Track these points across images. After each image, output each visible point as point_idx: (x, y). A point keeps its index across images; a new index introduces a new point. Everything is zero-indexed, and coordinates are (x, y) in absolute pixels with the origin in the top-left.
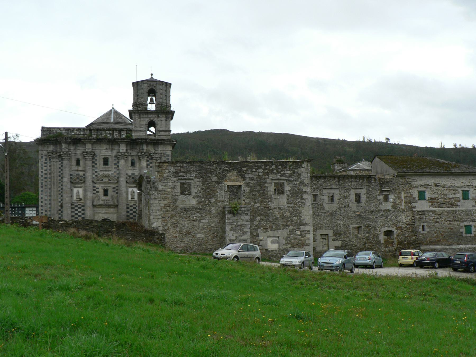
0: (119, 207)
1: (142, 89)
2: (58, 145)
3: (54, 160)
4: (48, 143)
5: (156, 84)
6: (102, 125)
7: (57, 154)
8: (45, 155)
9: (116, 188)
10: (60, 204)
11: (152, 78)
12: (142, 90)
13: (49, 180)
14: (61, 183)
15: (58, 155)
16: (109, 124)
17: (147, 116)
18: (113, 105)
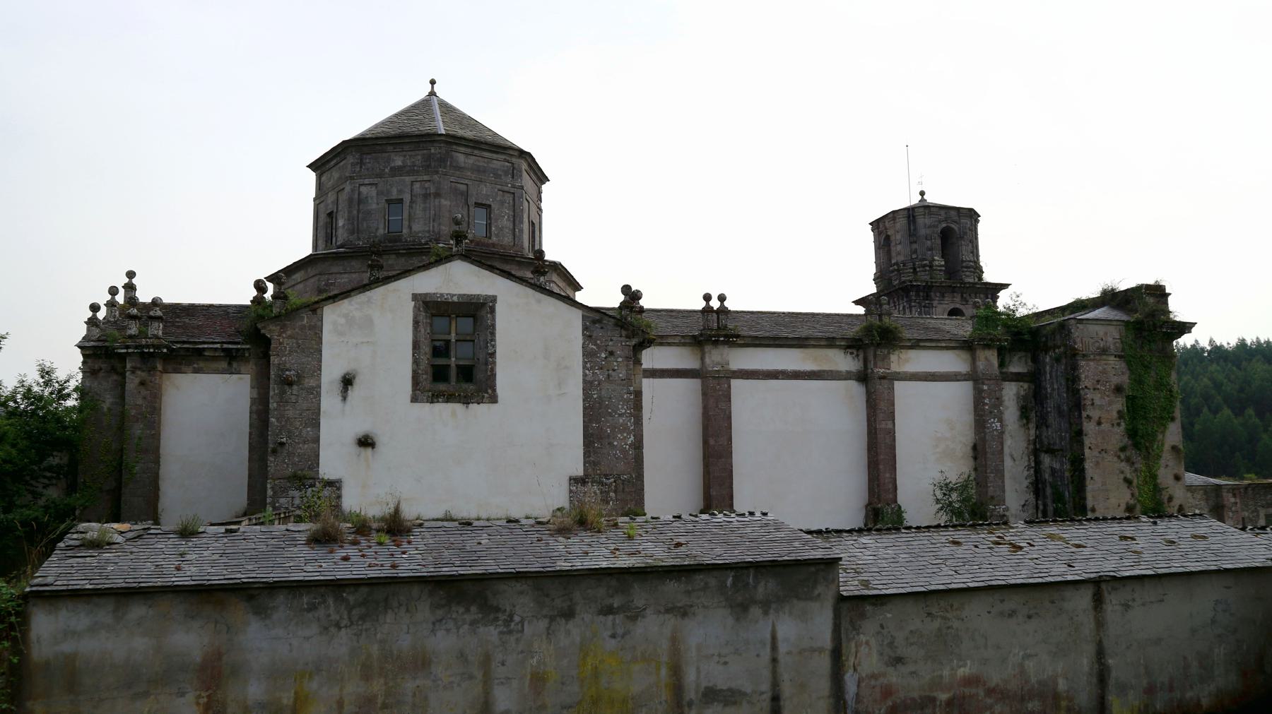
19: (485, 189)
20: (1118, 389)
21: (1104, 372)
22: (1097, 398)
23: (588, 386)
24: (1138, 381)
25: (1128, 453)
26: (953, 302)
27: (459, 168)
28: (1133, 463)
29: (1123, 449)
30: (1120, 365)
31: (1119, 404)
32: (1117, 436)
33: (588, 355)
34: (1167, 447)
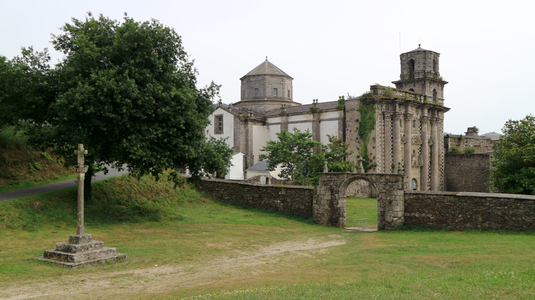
0: (423, 167)
1: (430, 58)
2: (389, 105)
3: (388, 120)
4: (384, 102)
5: (437, 56)
6: (275, 77)
7: (390, 114)
8: (380, 114)
9: (420, 150)
10: (391, 164)
11: (419, 48)
12: (430, 60)
13: (383, 139)
14: (392, 144)
15: (390, 115)
16: (282, 77)
17: (433, 84)
18: (267, 57)
19: (257, 85)
20: (357, 121)
21: (353, 116)
22: (350, 123)
23: (234, 129)
24: (363, 118)
25: (359, 140)
26: (410, 87)
27: (251, 82)
28: (360, 143)
29: (357, 139)
30: (358, 113)
31: (357, 125)
32: (356, 135)
33: (234, 123)
34: (371, 138)
